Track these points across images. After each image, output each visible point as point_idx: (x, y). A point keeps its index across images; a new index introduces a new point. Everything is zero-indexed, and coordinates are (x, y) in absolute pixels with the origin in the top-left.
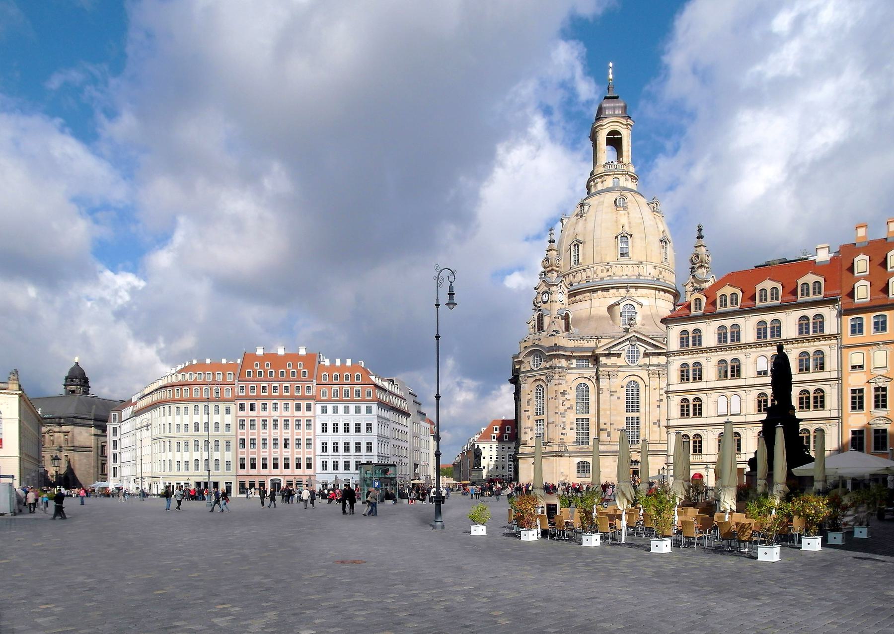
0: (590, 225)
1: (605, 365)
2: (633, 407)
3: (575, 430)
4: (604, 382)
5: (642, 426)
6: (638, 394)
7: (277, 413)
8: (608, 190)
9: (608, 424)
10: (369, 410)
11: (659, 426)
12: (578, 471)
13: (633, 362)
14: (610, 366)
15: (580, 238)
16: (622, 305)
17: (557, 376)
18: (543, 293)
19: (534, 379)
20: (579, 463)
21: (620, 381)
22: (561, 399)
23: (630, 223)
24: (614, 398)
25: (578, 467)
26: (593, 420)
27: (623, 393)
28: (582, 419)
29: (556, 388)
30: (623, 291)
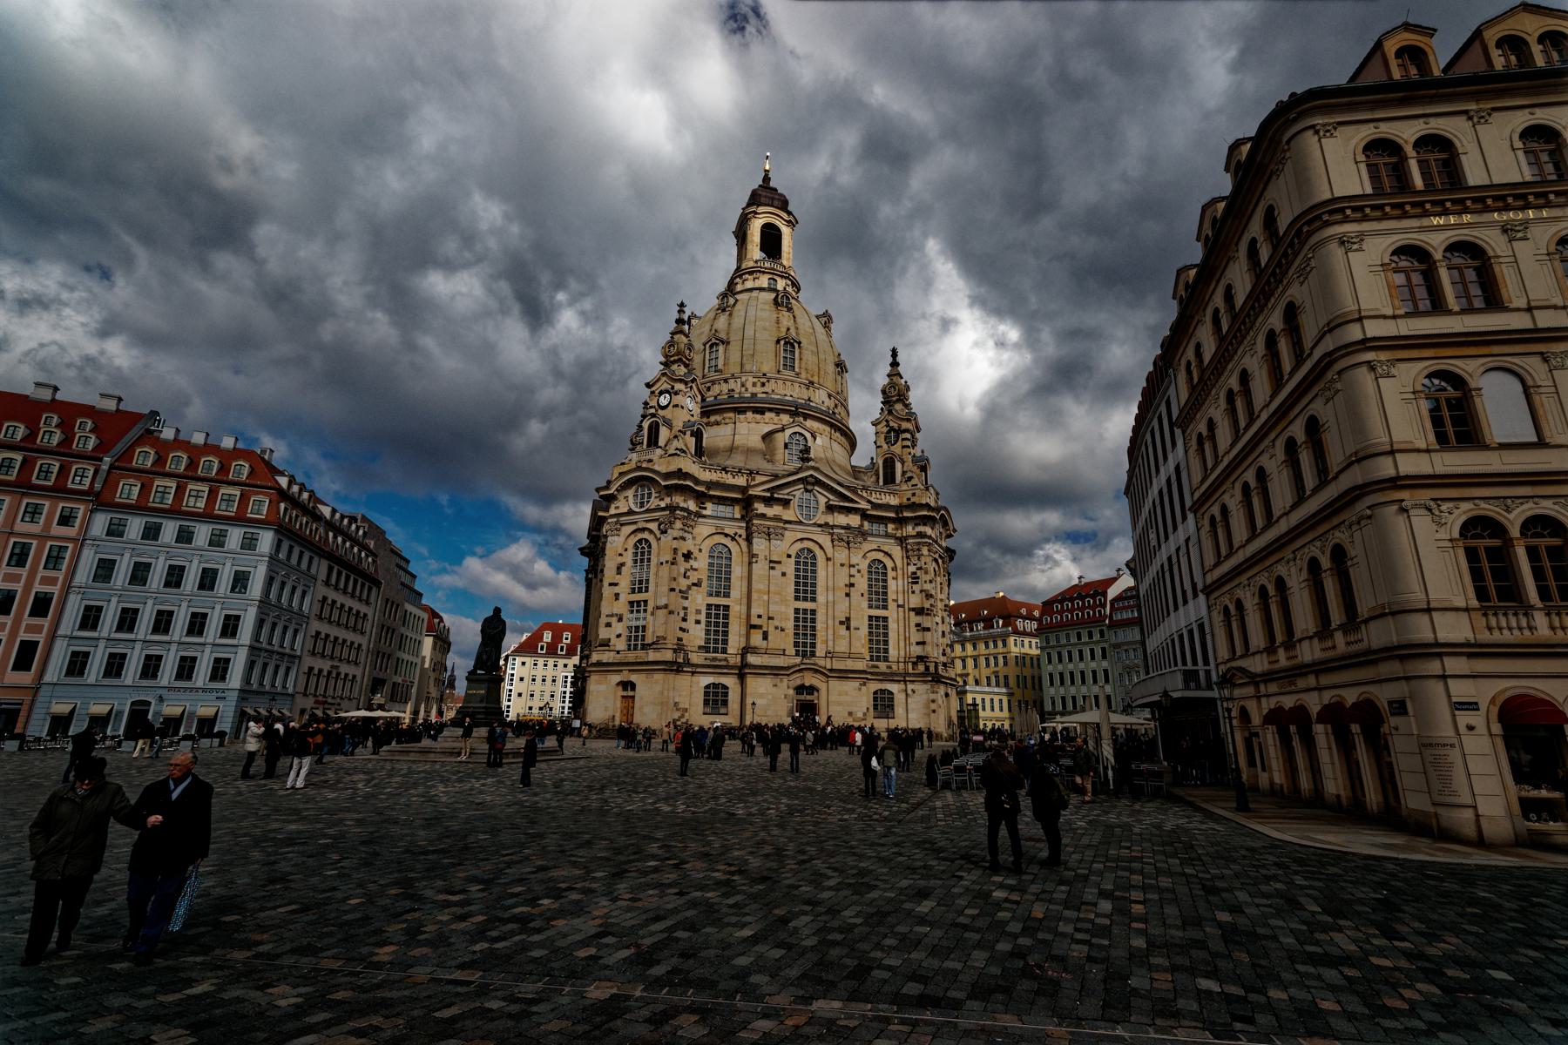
0: (737, 321)
1: (763, 516)
2: (805, 591)
3: (703, 625)
4: (759, 545)
5: (819, 626)
6: (814, 571)
8: (761, 289)
9: (765, 617)
10: (249, 544)
11: (848, 628)
12: (706, 702)
13: (809, 517)
14: (770, 519)
15: (723, 336)
16: (788, 432)
17: (678, 524)
18: (661, 393)
19: (634, 527)
20: (707, 687)
21: (786, 545)
22: (683, 565)
24: (776, 573)
25: (706, 694)
26: (737, 610)
27: (789, 567)
28: (718, 607)
29: (675, 544)
30: (786, 418)
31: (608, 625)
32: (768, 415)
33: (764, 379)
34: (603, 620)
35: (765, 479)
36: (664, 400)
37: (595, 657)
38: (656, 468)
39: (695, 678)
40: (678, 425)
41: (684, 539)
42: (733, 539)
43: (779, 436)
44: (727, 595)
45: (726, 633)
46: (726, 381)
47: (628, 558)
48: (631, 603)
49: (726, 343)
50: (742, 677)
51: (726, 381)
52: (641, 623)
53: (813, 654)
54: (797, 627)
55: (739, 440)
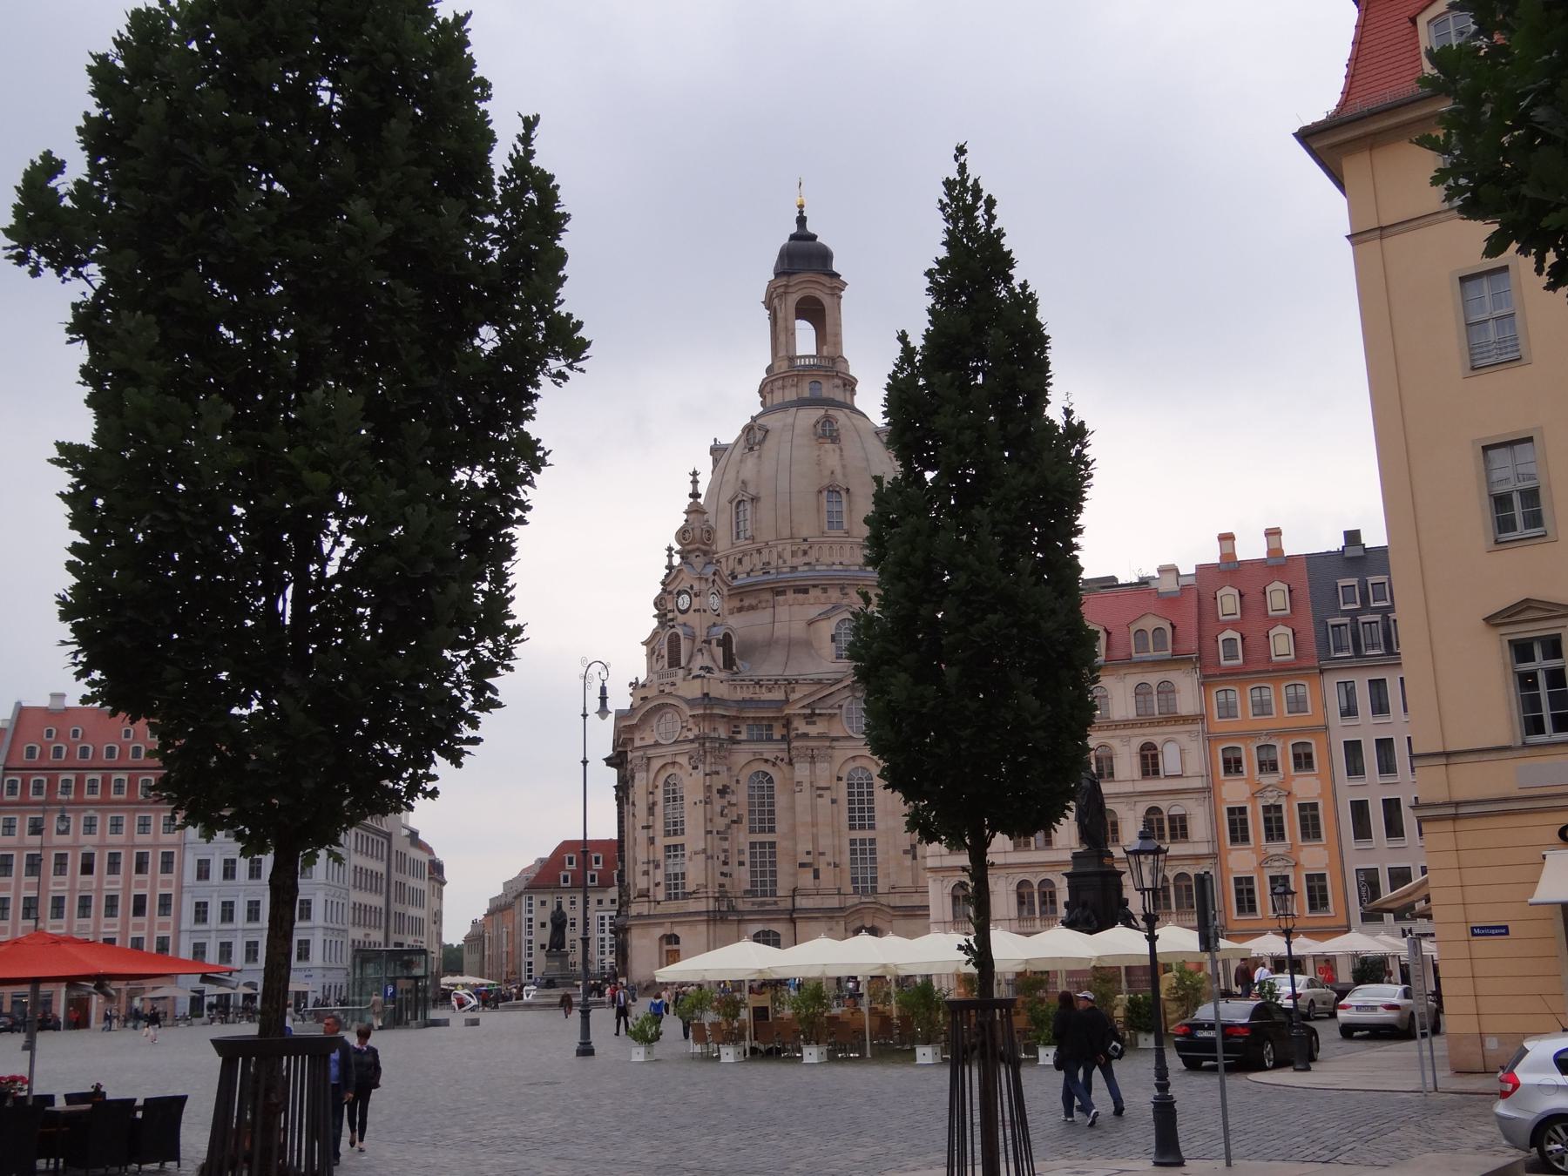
1: (805, 736)
2: (862, 818)
4: (802, 771)
5: (879, 856)
7: (93, 839)
11: (915, 857)
15: (752, 490)
18: (679, 594)
23: (844, 467)
24: (826, 800)
26: (783, 845)
27: (842, 791)
28: (762, 844)
30: (834, 595)
31: (646, 873)
32: (813, 593)
33: (805, 546)
34: (640, 868)
35: (806, 690)
36: (684, 601)
37: (634, 909)
38: (680, 693)
39: (743, 927)
40: (701, 634)
41: (717, 773)
42: (774, 764)
43: (824, 624)
44: (772, 830)
45: (773, 874)
46: (759, 551)
47: (660, 795)
48: (668, 848)
49: (755, 500)
50: (793, 921)
51: (759, 551)
52: (678, 870)
53: (874, 889)
54: (853, 861)
55: (781, 631)
